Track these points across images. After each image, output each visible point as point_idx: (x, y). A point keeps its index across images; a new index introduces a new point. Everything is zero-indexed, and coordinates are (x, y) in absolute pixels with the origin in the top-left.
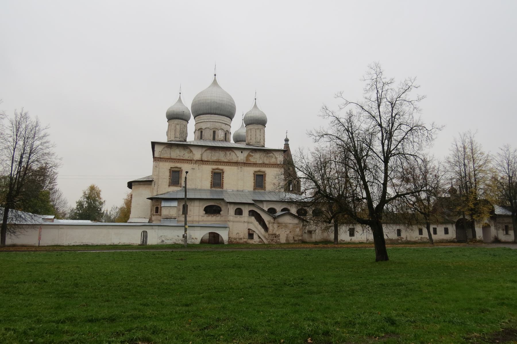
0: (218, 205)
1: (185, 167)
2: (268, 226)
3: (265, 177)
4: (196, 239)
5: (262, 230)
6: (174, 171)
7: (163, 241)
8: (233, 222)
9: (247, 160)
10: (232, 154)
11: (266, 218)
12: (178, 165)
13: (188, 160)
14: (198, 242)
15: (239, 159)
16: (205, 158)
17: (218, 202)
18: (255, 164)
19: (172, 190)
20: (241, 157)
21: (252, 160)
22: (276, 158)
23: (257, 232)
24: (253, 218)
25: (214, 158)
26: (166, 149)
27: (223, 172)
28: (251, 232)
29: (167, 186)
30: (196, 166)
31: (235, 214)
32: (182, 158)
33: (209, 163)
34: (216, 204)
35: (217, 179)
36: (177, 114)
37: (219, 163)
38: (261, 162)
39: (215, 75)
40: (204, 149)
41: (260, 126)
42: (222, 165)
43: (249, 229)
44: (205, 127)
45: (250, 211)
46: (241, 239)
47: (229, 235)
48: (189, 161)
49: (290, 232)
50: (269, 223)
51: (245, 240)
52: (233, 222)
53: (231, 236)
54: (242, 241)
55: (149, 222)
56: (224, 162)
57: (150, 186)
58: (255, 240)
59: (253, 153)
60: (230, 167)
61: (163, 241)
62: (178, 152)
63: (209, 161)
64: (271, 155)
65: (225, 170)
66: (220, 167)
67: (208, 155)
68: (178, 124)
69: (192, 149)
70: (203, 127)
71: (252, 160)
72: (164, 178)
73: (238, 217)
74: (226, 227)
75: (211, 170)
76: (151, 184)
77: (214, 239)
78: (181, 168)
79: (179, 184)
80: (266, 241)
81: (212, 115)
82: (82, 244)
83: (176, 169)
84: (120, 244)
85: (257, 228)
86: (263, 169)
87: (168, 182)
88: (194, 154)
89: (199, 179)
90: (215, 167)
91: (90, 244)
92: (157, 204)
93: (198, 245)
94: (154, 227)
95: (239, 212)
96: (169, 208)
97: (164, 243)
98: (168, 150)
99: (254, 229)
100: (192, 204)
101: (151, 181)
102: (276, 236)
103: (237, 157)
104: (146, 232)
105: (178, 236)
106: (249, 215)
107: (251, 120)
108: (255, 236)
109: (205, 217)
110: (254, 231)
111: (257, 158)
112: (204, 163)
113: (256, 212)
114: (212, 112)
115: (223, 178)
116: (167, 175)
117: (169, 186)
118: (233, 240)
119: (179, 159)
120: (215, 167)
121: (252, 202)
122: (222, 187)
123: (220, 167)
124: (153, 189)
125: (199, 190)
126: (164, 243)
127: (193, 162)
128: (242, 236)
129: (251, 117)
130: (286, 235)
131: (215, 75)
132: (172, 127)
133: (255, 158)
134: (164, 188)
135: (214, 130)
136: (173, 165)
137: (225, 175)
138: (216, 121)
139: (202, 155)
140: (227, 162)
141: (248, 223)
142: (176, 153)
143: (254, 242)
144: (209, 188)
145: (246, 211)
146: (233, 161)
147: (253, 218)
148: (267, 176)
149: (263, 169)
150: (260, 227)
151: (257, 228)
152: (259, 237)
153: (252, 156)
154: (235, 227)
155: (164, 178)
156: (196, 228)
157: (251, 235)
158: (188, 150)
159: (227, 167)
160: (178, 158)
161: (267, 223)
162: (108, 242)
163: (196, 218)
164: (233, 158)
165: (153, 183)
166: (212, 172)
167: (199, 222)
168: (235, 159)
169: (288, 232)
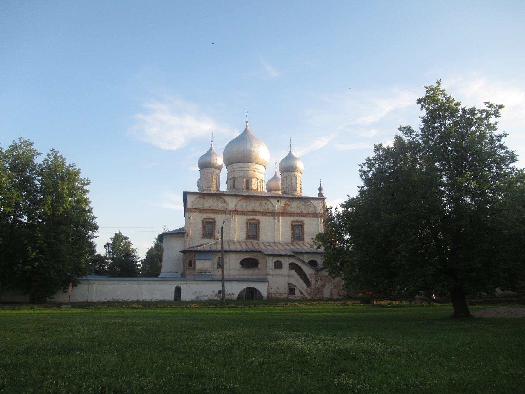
0: (256, 258)
1: (219, 218)
2: (310, 279)
3: (303, 227)
4: (233, 294)
5: (304, 285)
7: (197, 297)
8: (272, 275)
9: (284, 210)
12: (211, 216)
14: (236, 297)
16: (239, 208)
18: (292, 214)
20: (278, 206)
21: (289, 209)
22: (315, 207)
23: (298, 286)
25: (249, 208)
27: (259, 223)
31: (275, 267)
32: (215, 208)
34: (253, 257)
37: (254, 213)
38: (298, 211)
39: (247, 122)
40: (238, 199)
42: (258, 215)
43: (290, 284)
44: (238, 176)
45: (290, 264)
46: (281, 294)
47: (268, 290)
49: (335, 286)
51: (286, 295)
52: (272, 275)
53: (270, 291)
54: (282, 297)
55: (182, 277)
56: (259, 212)
58: (297, 296)
59: (290, 202)
60: (266, 217)
61: (197, 297)
62: (211, 202)
63: (244, 212)
64: (309, 203)
65: (260, 221)
66: (256, 217)
67: (242, 205)
69: (226, 198)
70: (236, 176)
71: (290, 210)
73: (278, 271)
74: (265, 282)
75: (245, 220)
77: (251, 295)
78: (214, 219)
83: (210, 220)
86: (301, 219)
87: (201, 234)
88: (227, 204)
89: (235, 231)
91: (121, 300)
95: (278, 265)
98: (201, 201)
99: (295, 284)
101: (184, 233)
103: (274, 206)
105: (214, 292)
106: (290, 269)
108: (297, 292)
110: (295, 286)
111: (294, 207)
113: (297, 265)
115: (259, 229)
117: (202, 238)
118: (273, 295)
121: (293, 254)
123: (256, 217)
126: (199, 299)
127: (227, 212)
128: (282, 292)
130: (330, 290)
131: (247, 122)
134: (196, 240)
136: (206, 216)
137: (261, 226)
139: (236, 204)
140: (263, 212)
142: (209, 203)
144: (245, 240)
145: (286, 262)
147: (293, 272)
148: (305, 226)
149: (301, 219)
150: (301, 281)
152: (301, 293)
153: (290, 205)
154: (276, 282)
156: (233, 283)
157: (292, 290)
158: (222, 200)
159: (262, 217)
160: (211, 208)
161: (308, 276)
163: (232, 272)
165: (185, 235)
166: (247, 223)
168: (271, 209)
169: (332, 287)
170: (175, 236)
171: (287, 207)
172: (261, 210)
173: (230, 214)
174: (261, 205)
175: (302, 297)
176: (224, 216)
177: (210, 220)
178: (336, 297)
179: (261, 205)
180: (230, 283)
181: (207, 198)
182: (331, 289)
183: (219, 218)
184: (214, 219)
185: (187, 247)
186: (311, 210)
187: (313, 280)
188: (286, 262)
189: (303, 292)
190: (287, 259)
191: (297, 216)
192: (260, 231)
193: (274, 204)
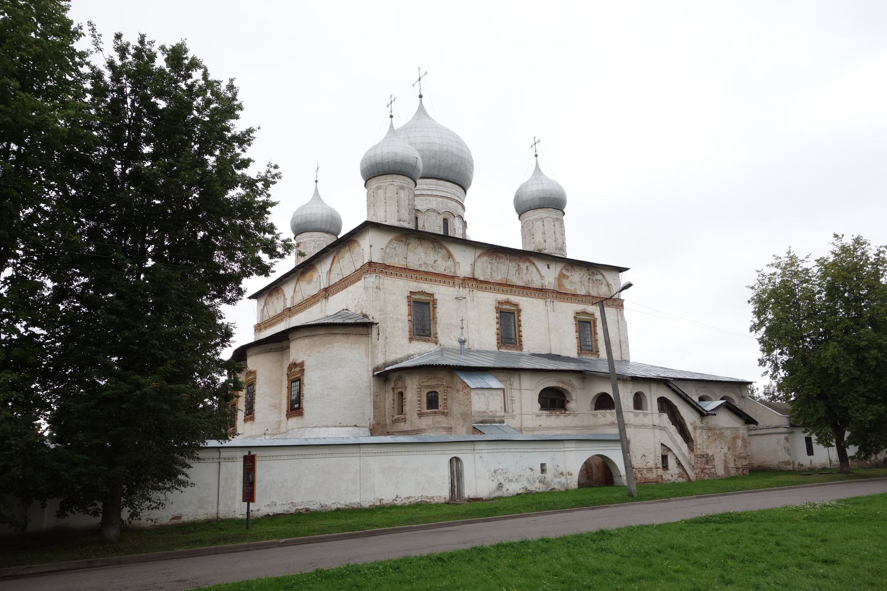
1: (443, 293)
5: (684, 446)
8: (636, 426)
9: (560, 285)
10: (532, 268)
11: (688, 415)
12: (427, 287)
13: (445, 276)
14: (573, 483)
15: (546, 283)
17: (566, 378)
18: (573, 297)
19: (417, 351)
21: (569, 287)
22: (608, 285)
23: (676, 452)
24: (665, 416)
25: (498, 277)
26: (395, 244)
27: (519, 311)
28: (665, 453)
29: (406, 341)
30: (463, 292)
32: (431, 270)
33: (488, 286)
34: (560, 385)
35: (508, 323)
36: (402, 163)
37: (509, 289)
38: (583, 292)
39: (421, 96)
40: (479, 252)
41: (553, 214)
46: (651, 469)
49: (729, 449)
50: (695, 429)
52: (636, 426)
56: (518, 287)
57: (364, 339)
61: (500, 486)
62: (423, 256)
64: (599, 277)
66: (514, 298)
67: (485, 269)
68: (402, 188)
72: (398, 320)
76: (368, 334)
78: (432, 295)
79: (429, 335)
80: (692, 475)
81: (441, 182)
82: (293, 510)
83: (423, 297)
84: (399, 502)
85: (674, 442)
87: (407, 329)
88: (456, 264)
90: (502, 297)
93: (575, 490)
94: (478, 447)
96: (487, 393)
97: (504, 490)
99: (669, 445)
100: (516, 385)
102: (708, 459)
103: (542, 277)
104: (457, 459)
105: (531, 469)
107: (544, 198)
108: (671, 462)
109: (544, 417)
110: (669, 450)
112: (480, 285)
114: (441, 175)
115: (520, 326)
116: (403, 310)
117: (411, 339)
119: (427, 273)
120: (502, 297)
122: (521, 350)
123: (514, 298)
124: (375, 346)
125: (477, 351)
127: (457, 281)
128: (651, 464)
129: (544, 191)
130: (723, 458)
131: (421, 96)
132: (388, 194)
133: (572, 283)
134: (399, 346)
135: (446, 216)
137: (523, 317)
138: (449, 195)
139: (473, 265)
140: (523, 288)
141: (663, 429)
142: (419, 256)
143: (670, 478)
144: (495, 348)
146: (534, 286)
150: (679, 438)
151: (674, 442)
152: (679, 464)
153: (568, 277)
155: (398, 320)
156: (567, 445)
158: (443, 252)
159: (524, 298)
160: (423, 269)
161: (690, 428)
162: (367, 500)
164: (535, 279)
167: (534, 429)
168: (537, 284)
169: (725, 450)
170: (344, 331)
171: (564, 281)
172: (520, 284)
173: (464, 287)
174: (519, 270)
175: (680, 476)
177: (423, 297)
178: (733, 472)
179: (519, 270)
180: (560, 445)
181: (414, 243)
182: (725, 455)
183: (443, 293)
184: (432, 295)
185: (380, 361)
186: (603, 291)
187: (698, 436)
188: (652, 395)
189: (684, 463)
190: (654, 387)
191: (582, 302)
192: (522, 329)
193: (543, 274)
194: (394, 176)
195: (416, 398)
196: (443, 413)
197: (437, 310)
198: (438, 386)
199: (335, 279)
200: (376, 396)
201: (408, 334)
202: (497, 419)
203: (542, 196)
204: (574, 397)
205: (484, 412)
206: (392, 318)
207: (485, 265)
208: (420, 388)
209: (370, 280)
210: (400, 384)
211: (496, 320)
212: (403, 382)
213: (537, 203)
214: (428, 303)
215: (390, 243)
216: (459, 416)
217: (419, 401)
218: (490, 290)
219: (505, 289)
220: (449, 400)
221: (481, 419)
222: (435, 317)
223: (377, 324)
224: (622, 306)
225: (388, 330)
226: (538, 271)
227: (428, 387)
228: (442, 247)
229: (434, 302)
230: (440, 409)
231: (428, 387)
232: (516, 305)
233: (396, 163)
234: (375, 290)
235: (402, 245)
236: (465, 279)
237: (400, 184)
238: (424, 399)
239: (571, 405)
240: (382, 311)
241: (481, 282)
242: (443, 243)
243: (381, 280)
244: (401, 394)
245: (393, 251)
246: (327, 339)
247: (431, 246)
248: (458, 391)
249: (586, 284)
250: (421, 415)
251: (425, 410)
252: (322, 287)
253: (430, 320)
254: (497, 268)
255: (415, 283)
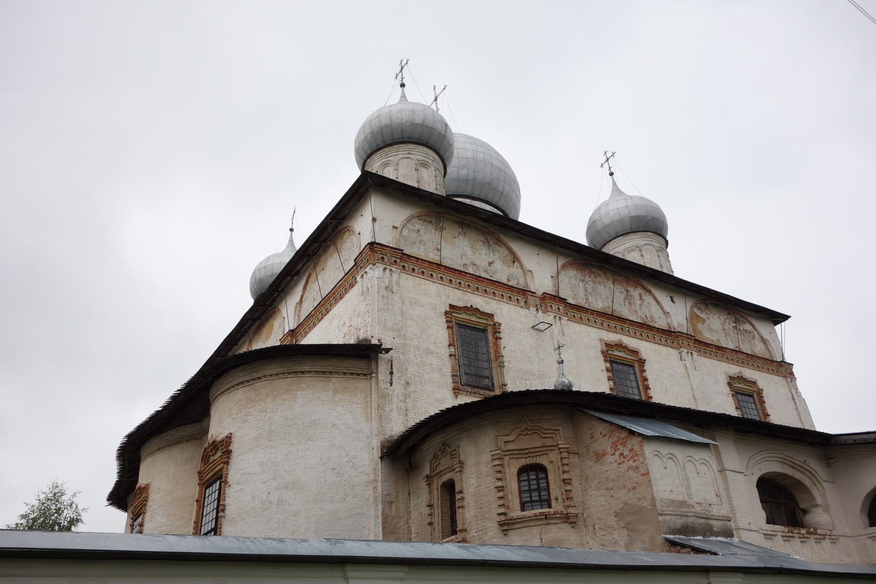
6: (461, 325)
10: (648, 298)
13: (510, 288)
15: (675, 324)
25: (599, 304)
26: (418, 225)
32: (483, 275)
33: (584, 316)
34: (789, 471)
37: (619, 325)
48: (519, 294)
57: (361, 384)
59: (702, 312)
60: (657, 347)
62: (469, 252)
68: (424, 165)
72: (429, 352)
75: (599, 347)
78: (491, 316)
83: (473, 319)
87: (448, 371)
88: (525, 272)
90: (613, 337)
92: (532, 442)
103: (666, 314)
109: (779, 540)
112: (572, 312)
114: (476, 195)
119: (478, 278)
124: (384, 396)
133: (712, 330)
139: (556, 278)
155: (429, 352)
164: (656, 316)
171: (700, 326)
174: (628, 297)
176: (524, 312)
177: (473, 319)
183: (510, 317)
185: (398, 427)
193: (667, 309)
194: (411, 146)
195: (490, 483)
196: (568, 519)
197: (503, 343)
198: (545, 450)
199: (308, 307)
200: (388, 503)
201: (450, 380)
202: (716, 525)
203: (634, 213)
204: (819, 501)
205: (683, 503)
206: (418, 347)
207: (573, 281)
208: (499, 458)
209: (374, 274)
210: (445, 463)
211: (606, 375)
212: (454, 455)
213: (628, 227)
214: (484, 331)
215: (409, 220)
216: (612, 521)
217: (500, 489)
218: (588, 323)
219: (612, 324)
220: (576, 483)
221: (679, 522)
222: (499, 356)
223: (388, 350)
224: (792, 374)
225: (411, 369)
226: (658, 303)
227: (521, 453)
228: (500, 242)
229: (496, 327)
230: (557, 506)
231: (521, 453)
232: (635, 352)
233: (414, 125)
234: (384, 293)
235: (431, 229)
236: (545, 297)
237: (420, 158)
238: (513, 485)
239: (818, 517)
240: (398, 330)
241: (572, 306)
242: (502, 236)
243: (395, 277)
244: (450, 489)
245: (414, 235)
246: (283, 383)
247: (482, 238)
248: (599, 457)
249: (732, 334)
250: (507, 525)
251: (516, 512)
252: (287, 330)
253: (489, 361)
254: (594, 289)
255: (457, 292)
